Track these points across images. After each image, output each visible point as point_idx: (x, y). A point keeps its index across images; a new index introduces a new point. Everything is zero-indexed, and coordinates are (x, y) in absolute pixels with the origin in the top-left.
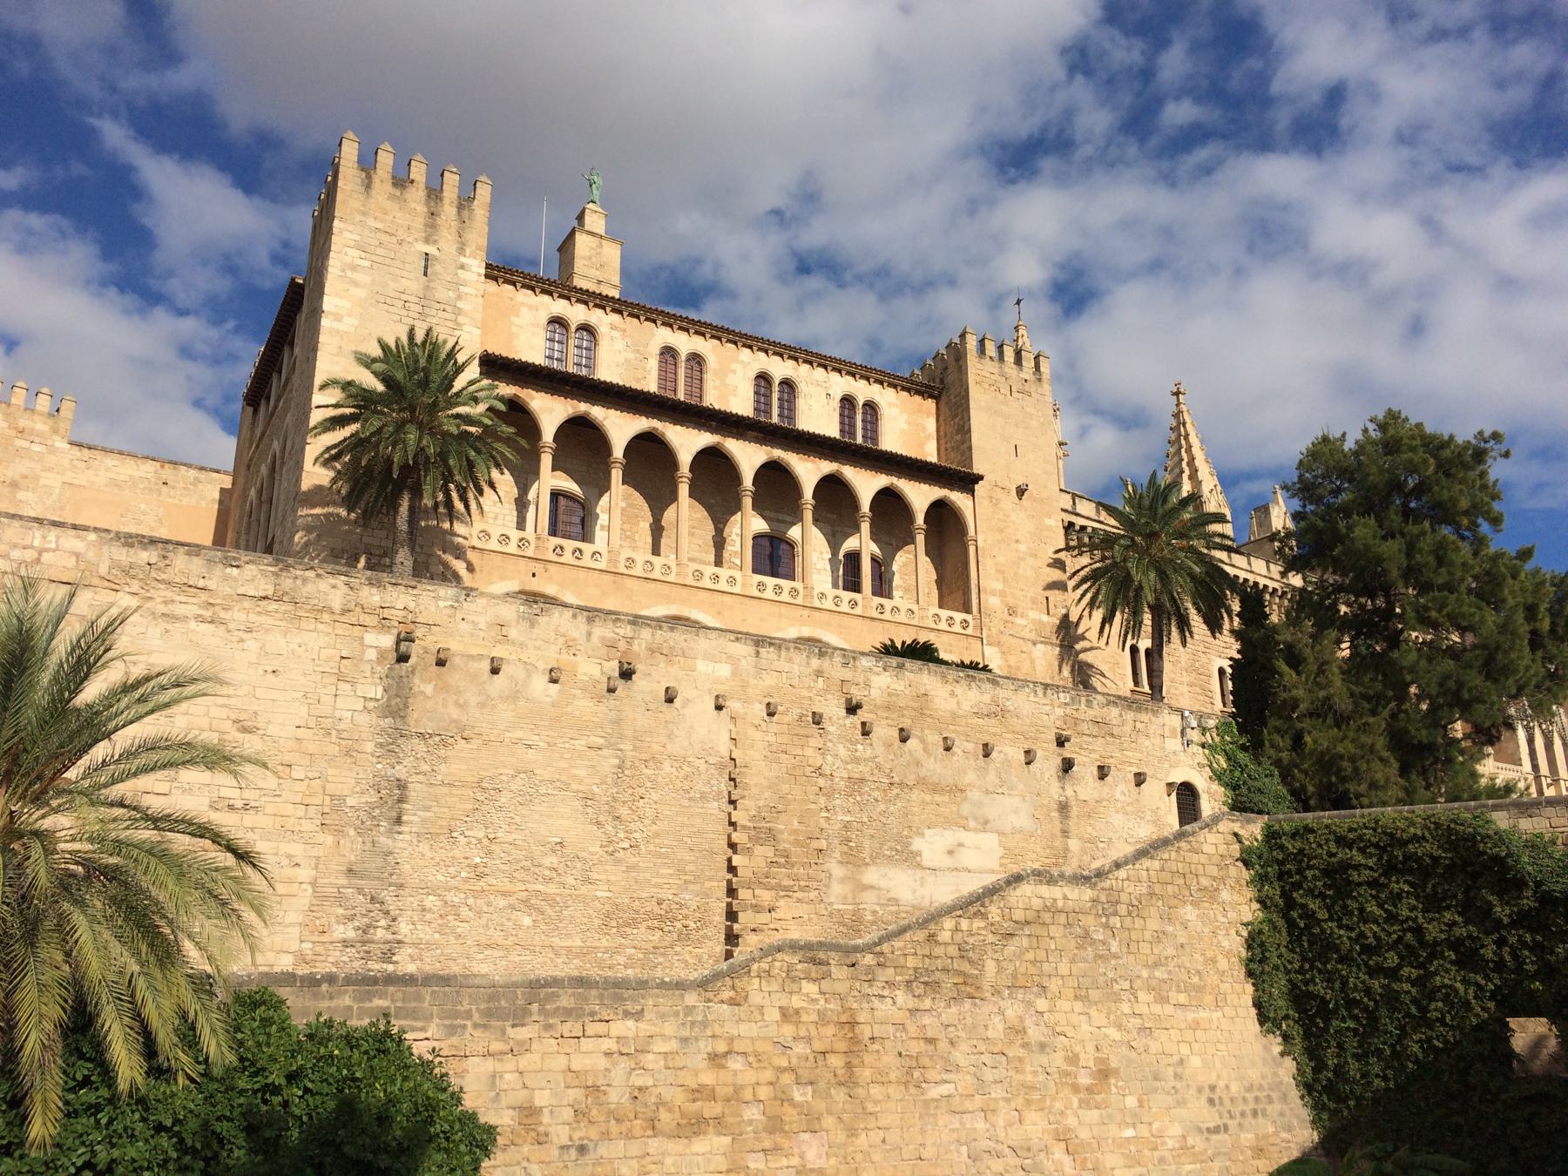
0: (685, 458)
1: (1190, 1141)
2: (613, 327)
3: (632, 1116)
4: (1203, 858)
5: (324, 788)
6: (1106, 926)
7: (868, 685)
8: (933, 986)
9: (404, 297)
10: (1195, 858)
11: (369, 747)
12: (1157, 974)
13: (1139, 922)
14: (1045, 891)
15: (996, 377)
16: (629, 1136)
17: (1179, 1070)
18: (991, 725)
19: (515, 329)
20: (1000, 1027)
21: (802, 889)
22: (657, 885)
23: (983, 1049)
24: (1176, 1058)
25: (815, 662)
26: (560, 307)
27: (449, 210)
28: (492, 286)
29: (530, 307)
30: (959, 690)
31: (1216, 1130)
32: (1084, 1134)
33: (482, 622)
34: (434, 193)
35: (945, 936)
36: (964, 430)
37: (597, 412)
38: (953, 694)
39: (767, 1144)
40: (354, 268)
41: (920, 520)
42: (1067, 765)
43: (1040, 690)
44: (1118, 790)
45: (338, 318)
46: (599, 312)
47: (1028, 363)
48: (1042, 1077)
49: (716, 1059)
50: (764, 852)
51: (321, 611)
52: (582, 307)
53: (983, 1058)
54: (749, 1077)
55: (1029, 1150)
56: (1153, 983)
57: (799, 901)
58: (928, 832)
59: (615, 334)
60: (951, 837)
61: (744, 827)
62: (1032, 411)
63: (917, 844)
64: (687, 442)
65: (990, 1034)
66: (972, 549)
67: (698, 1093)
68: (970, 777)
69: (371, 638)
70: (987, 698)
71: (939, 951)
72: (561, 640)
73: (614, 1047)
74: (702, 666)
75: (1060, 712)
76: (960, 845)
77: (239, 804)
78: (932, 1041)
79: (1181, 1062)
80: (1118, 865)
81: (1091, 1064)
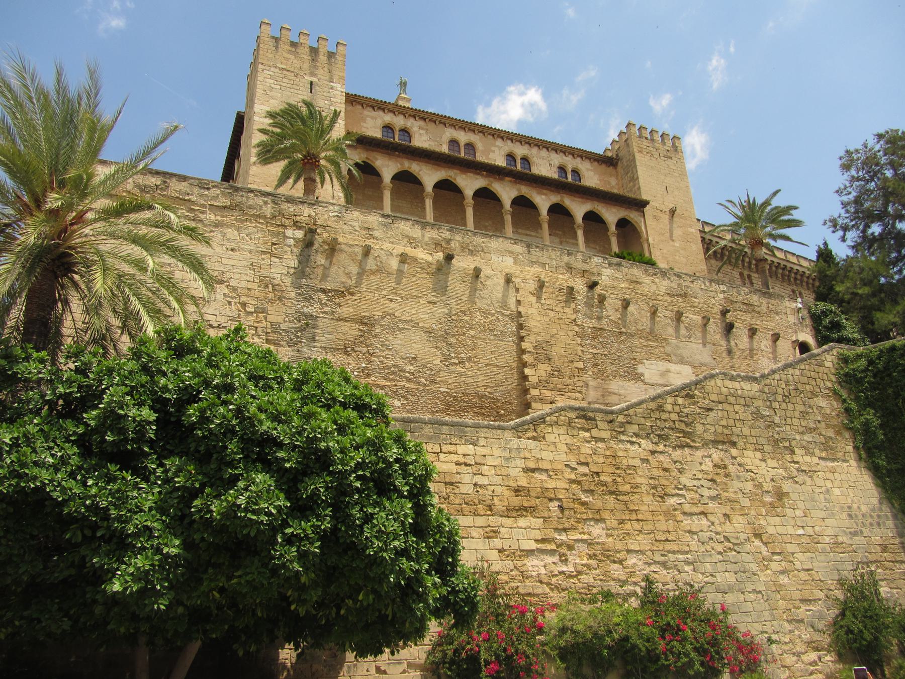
0: (469, 192)
1: (840, 539)
2: (420, 128)
3: (477, 502)
4: (826, 371)
5: (266, 318)
6: (770, 407)
7: (600, 274)
8: (662, 438)
10: (821, 369)
11: (293, 295)
12: (806, 438)
13: (790, 406)
14: (728, 383)
15: (651, 149)
16: (476, 514)
17: (827, 496)
18: (681, 303)
20: (711, 464)
21: (573, 391)
22: (477, 386)
23: (700, 477)
24: (824, 489)
25: (566, 258)
26: (388, 118)
27: (322, 58)
28: (350, 108)
29: (372, 118)
30: (657, 280)
31: (855, 534)
32: (771, 530)
34: (314, 51)
35: (669, 407)
36: (634, 179)
37: (415, 167)
38: (653, 282)
39: (567, 525)
41: (613, 228)
42: (729, 328)
43: (707, 282)
44: (762, 344)
46: (412, 120)
47: (669, 143)
48: (740, 495)
49: (526, 470)
50: (544, 369)
51: (259, 216)
52: (401, 117)
53: (702, 482)
54: (551, 484)
55: (737, 538)
56: (804, 443)
57: (569, 398)
58: (645, 361)
59: (421, 131)
60: (663, 366)
61: (530, 352)
63: (640, 369)
64: (469, 184)
65: (703, 467)
66: (645, 246)
67: (517, 491)
69: (289, 232)
70: (675, 285)
71: (664, 416)
72: (406, 240)
73: (462, 460)
75: (721, 296)
76: (668, 371)
77: (215, 324)
78: (665, 470)
79: (828, 491)
80: (774, 372)
81: (771, 489)
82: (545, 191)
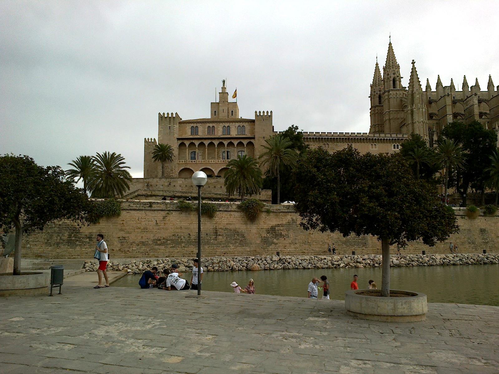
0: (206, 145)
26: (192, 125)
27: (172, 119)
29: (189, 126)
33: (155, 181)
37: (193, 141)
40: (161, 131)
68: (213, 190)
69: (145, 184)
74: (178, 182)
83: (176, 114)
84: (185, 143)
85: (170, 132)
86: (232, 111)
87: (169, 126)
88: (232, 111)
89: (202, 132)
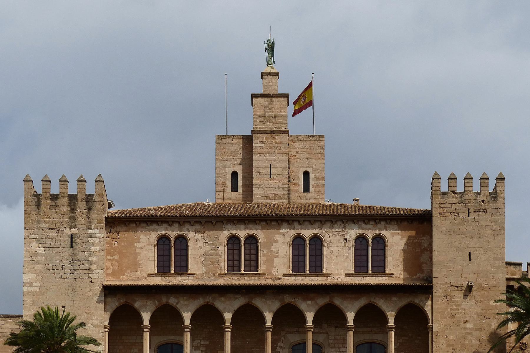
9: (62, 263)
19: (138, 250)
27: (81, 205)
37: (172, 301)
40: (36, 254)
45: (31, 284)
46: (187, 226)
52: (176, 225)
62: (488, 223)
82: (312, 295)
83: (99, 181)
84: (137, 305)
85: (73, 260)
86: (306, 174)
87: (69, 231)
88: (306, 174)
89: (206, 259)
